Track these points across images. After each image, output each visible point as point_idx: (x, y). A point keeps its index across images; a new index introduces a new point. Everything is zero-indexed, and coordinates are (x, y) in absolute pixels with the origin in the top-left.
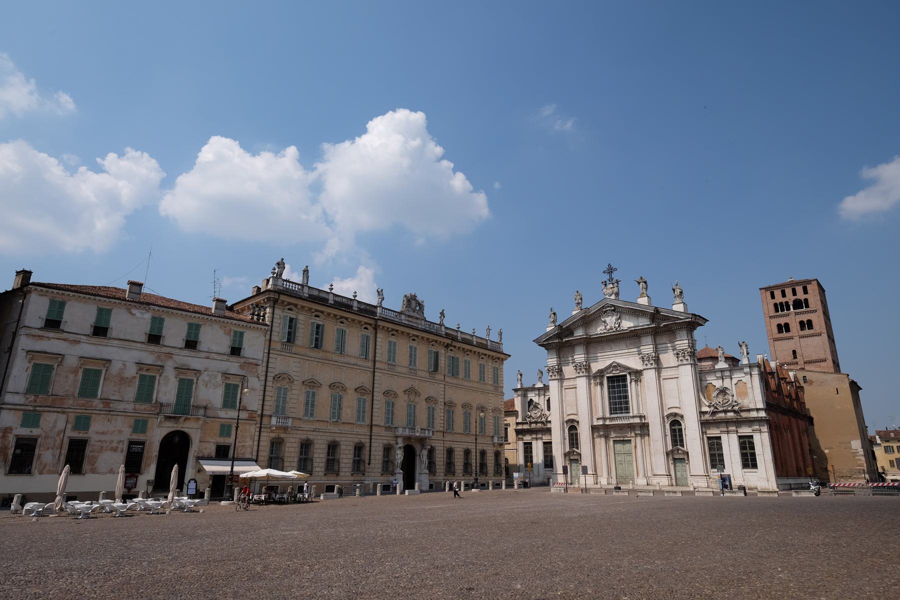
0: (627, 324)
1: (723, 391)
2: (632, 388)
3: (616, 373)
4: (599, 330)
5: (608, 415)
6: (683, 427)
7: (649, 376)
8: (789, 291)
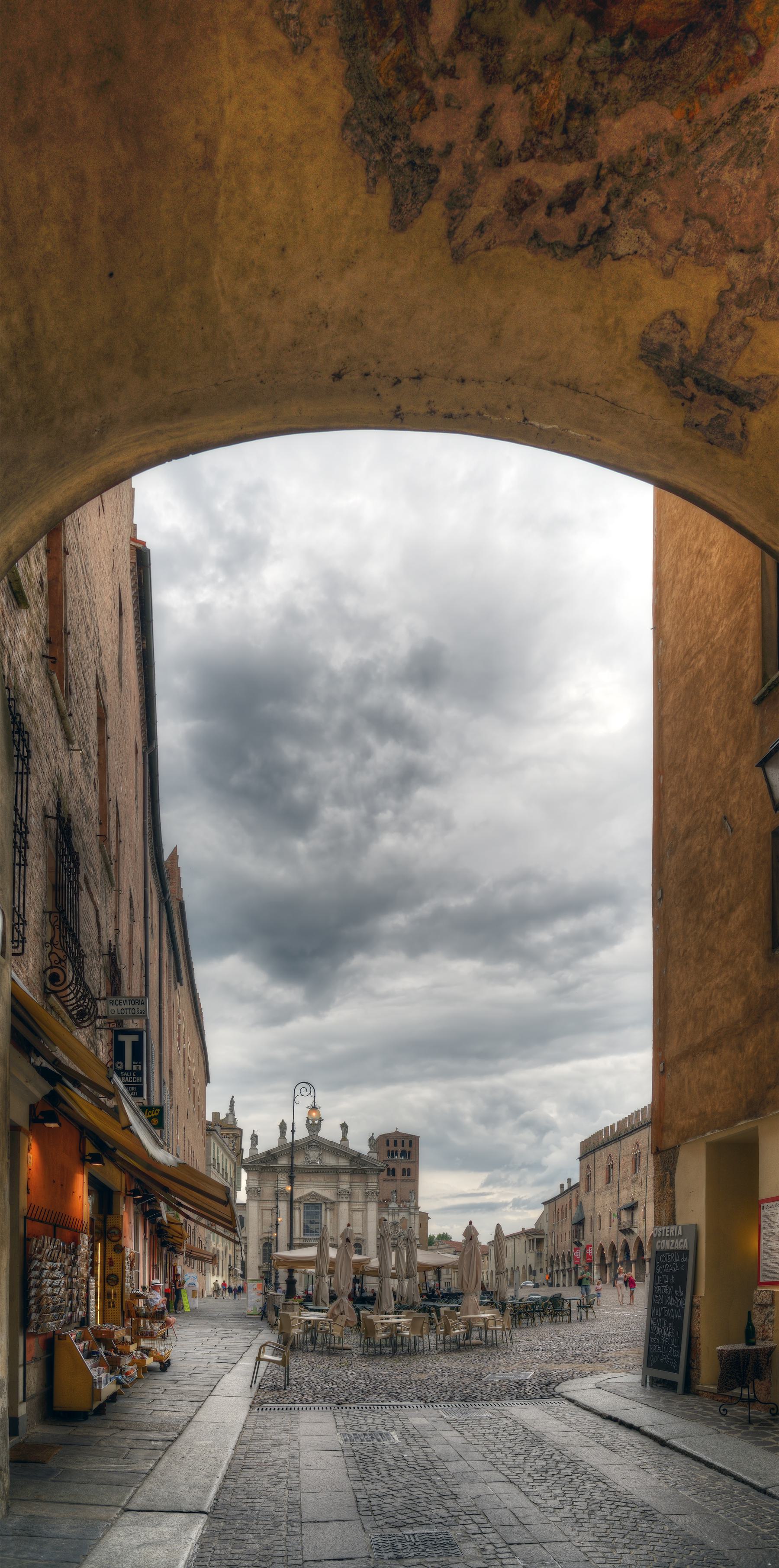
0: (330, 1161)
1: (395, 1224)
2: (327, 1218)
3: (313, 1201)
4: (299, 1161)
5: (302, 1236)
6: (363, 1248)
7: (344, 1207)
8: (399, 1143)
